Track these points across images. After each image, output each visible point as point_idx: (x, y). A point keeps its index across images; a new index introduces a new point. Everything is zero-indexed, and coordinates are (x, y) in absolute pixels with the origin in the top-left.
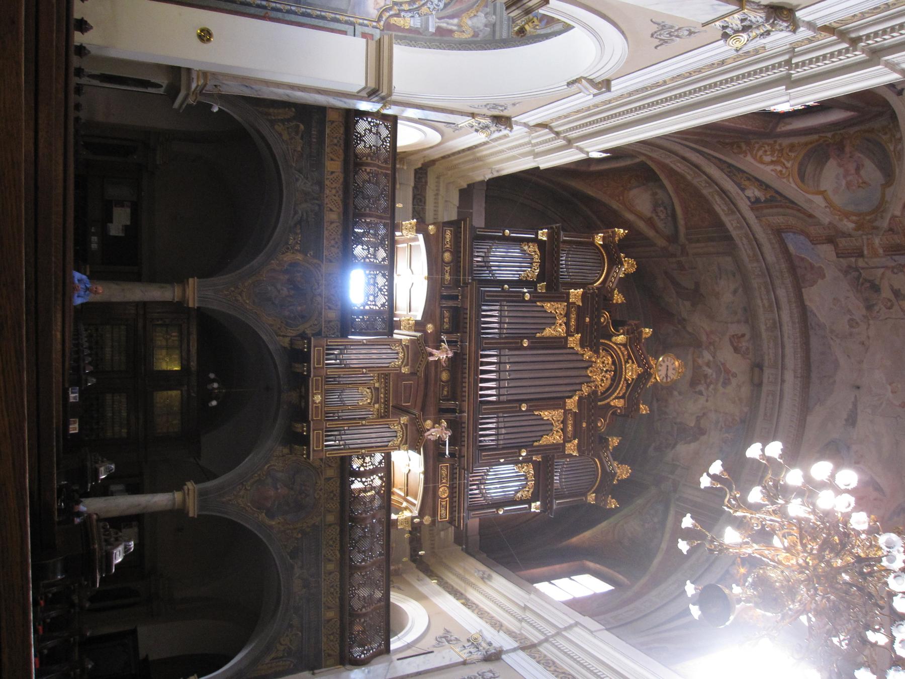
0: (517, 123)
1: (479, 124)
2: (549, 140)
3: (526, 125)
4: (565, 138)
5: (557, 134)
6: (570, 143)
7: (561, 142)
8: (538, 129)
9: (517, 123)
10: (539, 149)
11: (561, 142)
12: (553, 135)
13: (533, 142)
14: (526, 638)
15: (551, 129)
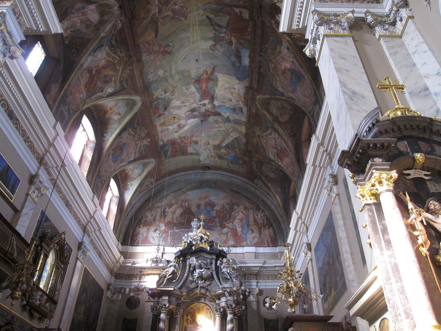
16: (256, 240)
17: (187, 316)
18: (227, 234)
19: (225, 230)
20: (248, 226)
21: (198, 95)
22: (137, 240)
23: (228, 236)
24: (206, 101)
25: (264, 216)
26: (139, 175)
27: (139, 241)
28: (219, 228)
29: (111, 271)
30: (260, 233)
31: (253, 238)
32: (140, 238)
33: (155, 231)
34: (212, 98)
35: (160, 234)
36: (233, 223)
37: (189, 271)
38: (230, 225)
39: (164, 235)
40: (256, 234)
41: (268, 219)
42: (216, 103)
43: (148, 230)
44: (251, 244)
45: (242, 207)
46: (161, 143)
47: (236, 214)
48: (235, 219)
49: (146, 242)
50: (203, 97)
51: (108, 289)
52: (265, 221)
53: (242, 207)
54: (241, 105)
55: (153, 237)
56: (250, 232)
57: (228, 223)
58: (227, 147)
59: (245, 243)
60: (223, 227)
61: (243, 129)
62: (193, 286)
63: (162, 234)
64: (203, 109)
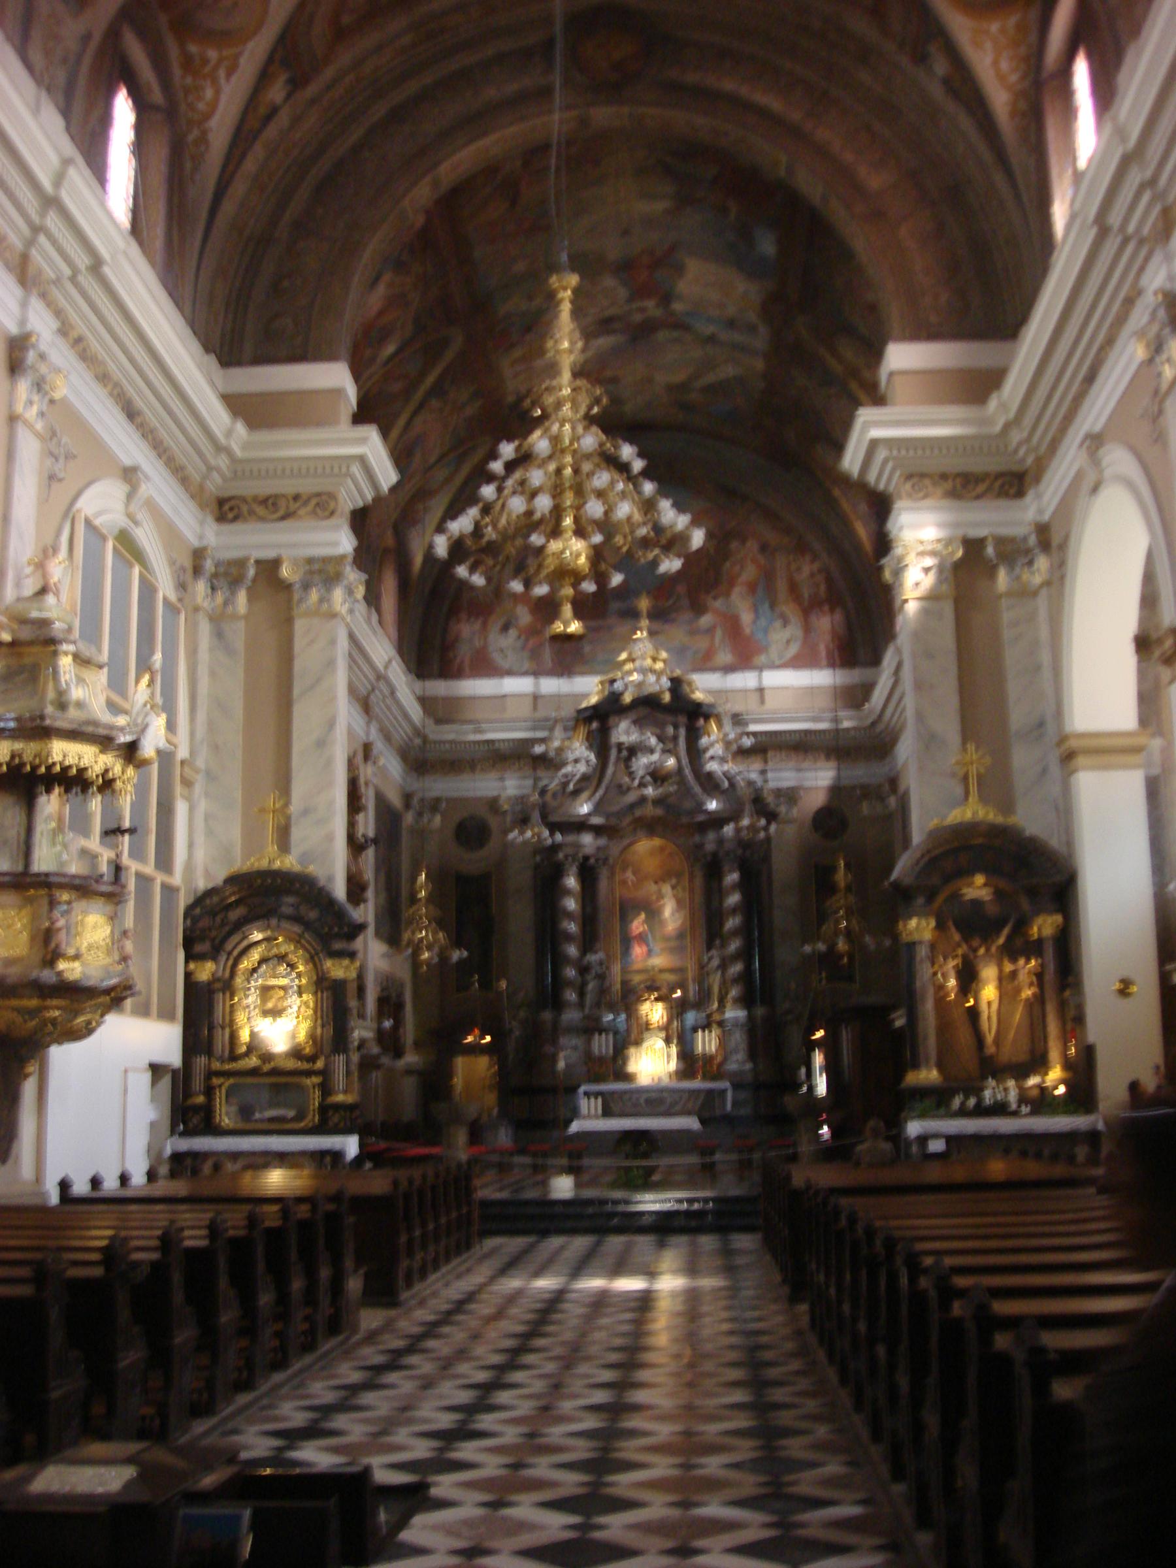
0: (23, 322)
1: (30, 403)
2: (54, 242)
3: (24, 305)
4: (43, 215)
5: (36, 229)
6: (51, 202)
7: (52, 221)
8: (31, 271)
9: (23, 322)
10: (82, 261)
11: (52, 221)
12: (42, 239)
13: (67, 271)
14: (1154, 225)
15: (30, 243)
16: (794, 649)
17: (624, 869)
18: (710, 631)
19: (706, 620)
20: (772, 606)
21: (622, 293)
22: (458, 661)
23: (713, 637)
24: (650, 304)
25: (820, 571)
26: (448, 480)
27: (462, 662)
28: (687, 616)
29: (405, 754)
30: (807, 629)
31: (788, 642)
32: (464, 652)
33: (505, 628)
34: (666, 299)
35: (519, 637)
36: (728, 594)
37: (618, 759)
38: (718, 604)
39: (531, 642)
40: (794, 630)
41: (829, 581)
42: (677, 306)
43: (485, 625)
44: (782, 662)
45: (752, 545)
46: (510, 399)
47: (737, 568)
48: (732, 583)
49: (485, 666)
50: (640, 292)
51: (407, 806)
52: (823, 588)
53: (752, 545)
54: (752, 317)
55: (502, 650)
56: (778, 624)
57: (715, 598)
58: (709, 389)
59: (762, 659)
60: (699, 609)
61: (759, 365)
62: (631, 797)
63: (527, 640)
64: (638, 318)
